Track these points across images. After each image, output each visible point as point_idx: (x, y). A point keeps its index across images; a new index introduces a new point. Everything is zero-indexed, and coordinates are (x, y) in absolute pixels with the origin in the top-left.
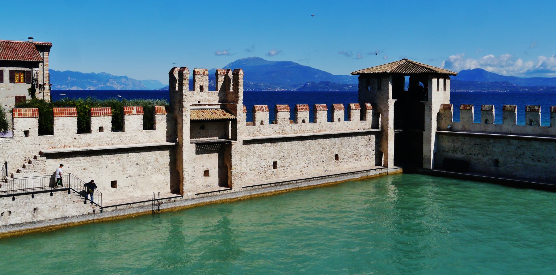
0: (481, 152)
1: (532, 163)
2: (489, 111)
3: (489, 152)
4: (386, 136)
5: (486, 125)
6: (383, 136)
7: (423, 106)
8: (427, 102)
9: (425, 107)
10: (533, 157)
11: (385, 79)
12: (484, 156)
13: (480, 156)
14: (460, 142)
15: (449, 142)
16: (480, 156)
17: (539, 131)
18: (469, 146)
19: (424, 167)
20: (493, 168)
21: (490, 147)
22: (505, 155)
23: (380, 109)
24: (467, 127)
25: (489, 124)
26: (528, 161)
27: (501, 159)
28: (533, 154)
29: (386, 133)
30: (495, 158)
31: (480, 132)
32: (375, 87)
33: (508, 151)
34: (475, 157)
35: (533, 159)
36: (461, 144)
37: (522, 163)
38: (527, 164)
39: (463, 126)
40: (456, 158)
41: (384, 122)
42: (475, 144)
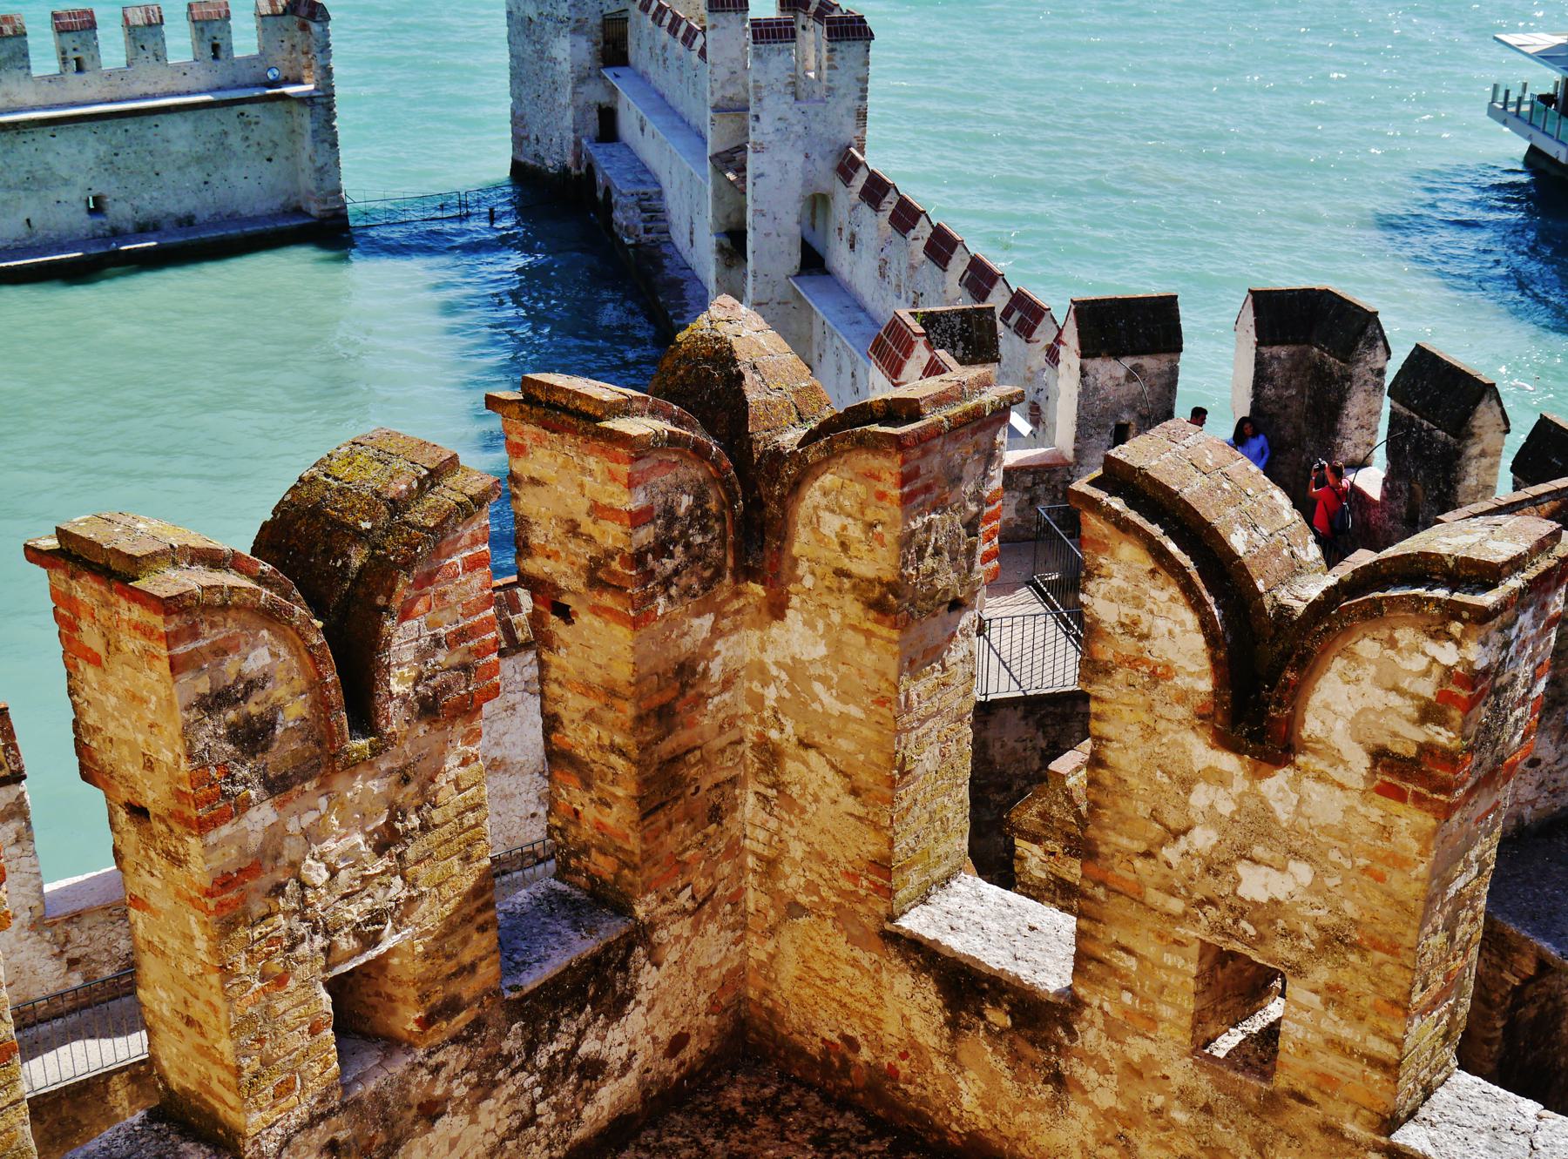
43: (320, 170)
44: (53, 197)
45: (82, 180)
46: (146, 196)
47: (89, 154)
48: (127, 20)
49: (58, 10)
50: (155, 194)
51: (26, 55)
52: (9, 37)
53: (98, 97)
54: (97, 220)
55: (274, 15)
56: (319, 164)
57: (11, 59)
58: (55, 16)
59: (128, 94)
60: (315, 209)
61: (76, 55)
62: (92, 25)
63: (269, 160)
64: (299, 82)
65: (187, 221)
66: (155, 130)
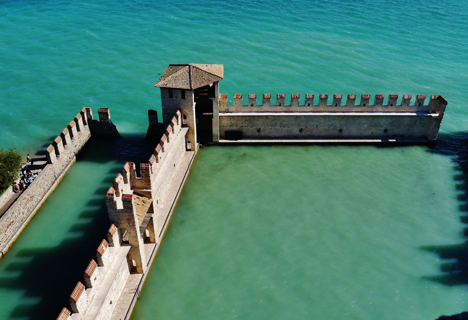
0: (249, 125)
1: (281, 129)
2: (254, 98)
3: (254, 124)
4: (192, 131)
5: (252, 107)
6: (190, 131)
7: (211, 102)
8: (214, 99)
9: (213, 102)
10: (281, 125)
11: (189, 92)
12: (251, 127)
13: (249, 127)
14: (235, 120)
15: (227, 120)
16: (249, 127)
17: (284, 109)
18: (241, 122)
19: (213, 141)
20: (257, 134)
21: (255, 121)
22: (265, 125)
23: (185, 112)
24: (239, 109)
25: (254, 106)
26: (278, 128)
27: (262, 128)
28: (281, 123)
29: (192, 129)
30: (259, 127)
31: (247, 112)
32: (178, 96)
33: (266, 123)
34: (245, 128)
35: (281, 126)
36: (236, 121)
37: (275, 129)
38: (278, 129)
39: (236, 109)
40: (233, 130)
41: (190, 122)
42: (246, 120)
43: (434, 132)
44: (378, 128)
45: (385, 126)
46: (396, 130)
47: (388, 122)
48: (404, 97)
49: (391, 94)
50: (398, 130)
51: (382, 102)
52: (381, 99)
53: (393, 111)
54: (385, 133)
55: (435, 99)
56: (434, 131)
57: (379, 103)
58: (390, 95)
59: (399, 111)
60: (429, 138)
61: (392, 103)
62: (397, 98)
63: (423, 127)
64: (435, 113)
65: (402, 136)
66: (402, 119)
